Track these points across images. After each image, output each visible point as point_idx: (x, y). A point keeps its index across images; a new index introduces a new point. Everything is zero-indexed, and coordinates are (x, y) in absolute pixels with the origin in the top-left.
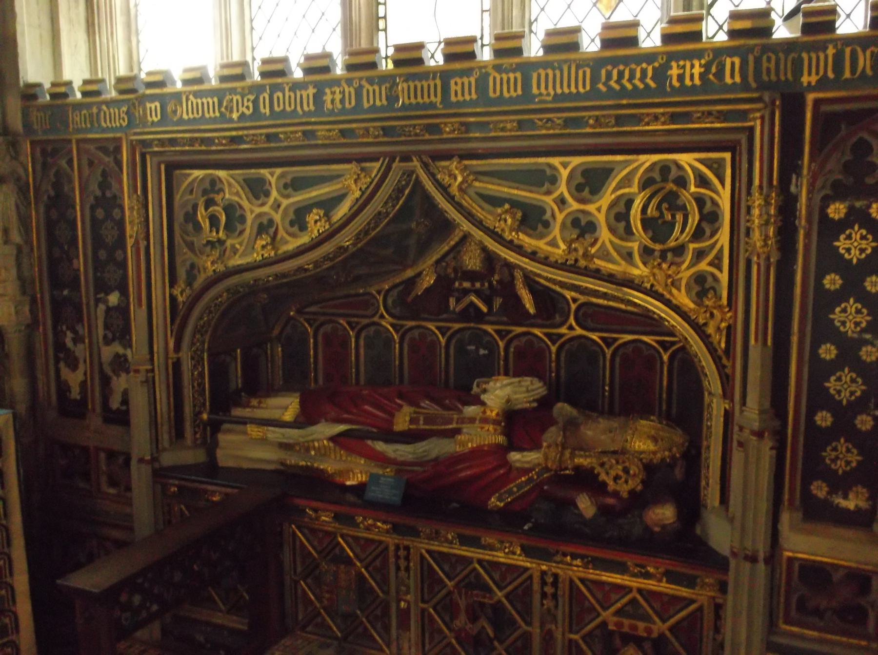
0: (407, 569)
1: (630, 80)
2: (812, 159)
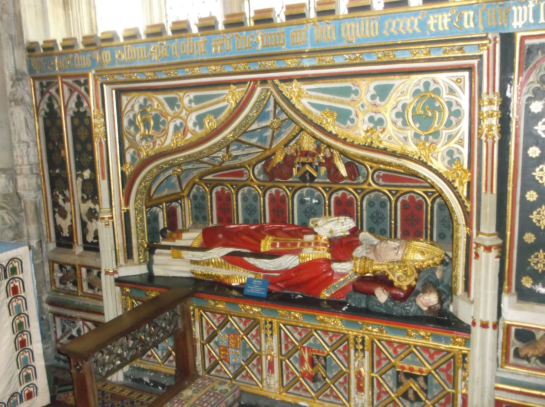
1: (404, 28)
2: (519, 75)
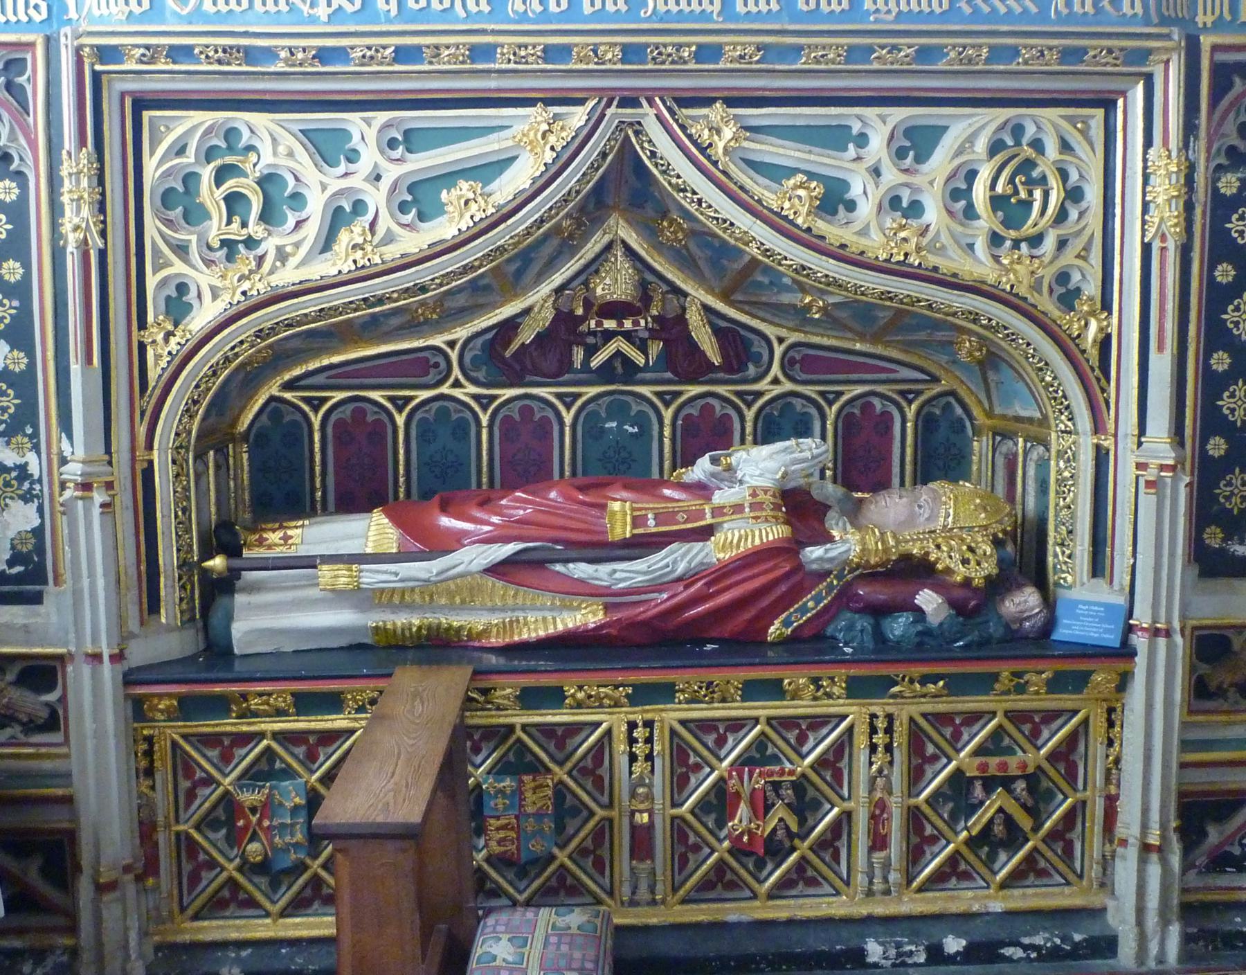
0: (649, 757)
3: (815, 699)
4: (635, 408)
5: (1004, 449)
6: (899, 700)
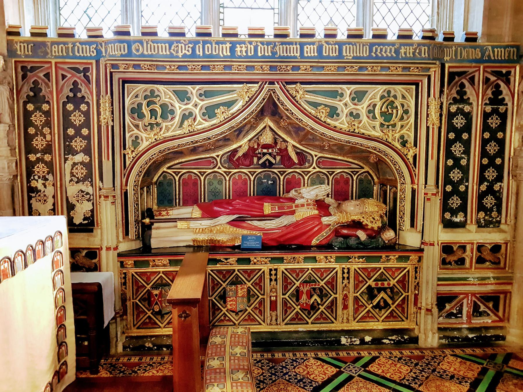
0: (276, 280)
1: (385, 52)
2: (447, 89)
3: (326, 263)
4: (272, 176)
5: (383, 189)
6: (351, 264)
